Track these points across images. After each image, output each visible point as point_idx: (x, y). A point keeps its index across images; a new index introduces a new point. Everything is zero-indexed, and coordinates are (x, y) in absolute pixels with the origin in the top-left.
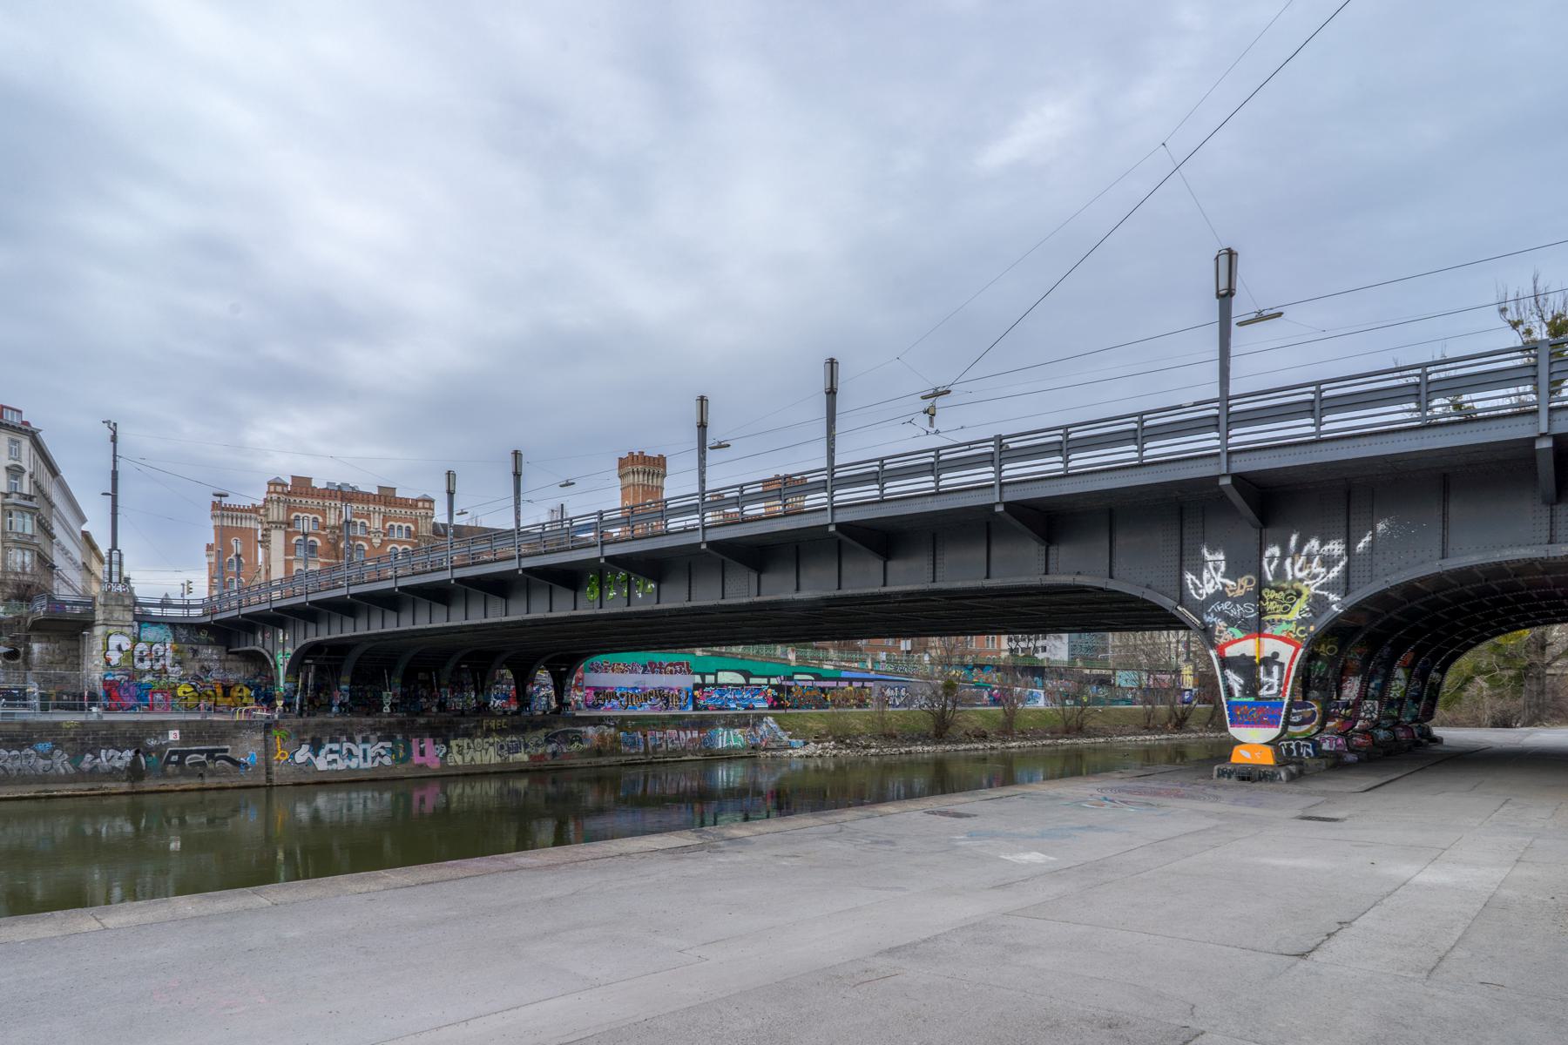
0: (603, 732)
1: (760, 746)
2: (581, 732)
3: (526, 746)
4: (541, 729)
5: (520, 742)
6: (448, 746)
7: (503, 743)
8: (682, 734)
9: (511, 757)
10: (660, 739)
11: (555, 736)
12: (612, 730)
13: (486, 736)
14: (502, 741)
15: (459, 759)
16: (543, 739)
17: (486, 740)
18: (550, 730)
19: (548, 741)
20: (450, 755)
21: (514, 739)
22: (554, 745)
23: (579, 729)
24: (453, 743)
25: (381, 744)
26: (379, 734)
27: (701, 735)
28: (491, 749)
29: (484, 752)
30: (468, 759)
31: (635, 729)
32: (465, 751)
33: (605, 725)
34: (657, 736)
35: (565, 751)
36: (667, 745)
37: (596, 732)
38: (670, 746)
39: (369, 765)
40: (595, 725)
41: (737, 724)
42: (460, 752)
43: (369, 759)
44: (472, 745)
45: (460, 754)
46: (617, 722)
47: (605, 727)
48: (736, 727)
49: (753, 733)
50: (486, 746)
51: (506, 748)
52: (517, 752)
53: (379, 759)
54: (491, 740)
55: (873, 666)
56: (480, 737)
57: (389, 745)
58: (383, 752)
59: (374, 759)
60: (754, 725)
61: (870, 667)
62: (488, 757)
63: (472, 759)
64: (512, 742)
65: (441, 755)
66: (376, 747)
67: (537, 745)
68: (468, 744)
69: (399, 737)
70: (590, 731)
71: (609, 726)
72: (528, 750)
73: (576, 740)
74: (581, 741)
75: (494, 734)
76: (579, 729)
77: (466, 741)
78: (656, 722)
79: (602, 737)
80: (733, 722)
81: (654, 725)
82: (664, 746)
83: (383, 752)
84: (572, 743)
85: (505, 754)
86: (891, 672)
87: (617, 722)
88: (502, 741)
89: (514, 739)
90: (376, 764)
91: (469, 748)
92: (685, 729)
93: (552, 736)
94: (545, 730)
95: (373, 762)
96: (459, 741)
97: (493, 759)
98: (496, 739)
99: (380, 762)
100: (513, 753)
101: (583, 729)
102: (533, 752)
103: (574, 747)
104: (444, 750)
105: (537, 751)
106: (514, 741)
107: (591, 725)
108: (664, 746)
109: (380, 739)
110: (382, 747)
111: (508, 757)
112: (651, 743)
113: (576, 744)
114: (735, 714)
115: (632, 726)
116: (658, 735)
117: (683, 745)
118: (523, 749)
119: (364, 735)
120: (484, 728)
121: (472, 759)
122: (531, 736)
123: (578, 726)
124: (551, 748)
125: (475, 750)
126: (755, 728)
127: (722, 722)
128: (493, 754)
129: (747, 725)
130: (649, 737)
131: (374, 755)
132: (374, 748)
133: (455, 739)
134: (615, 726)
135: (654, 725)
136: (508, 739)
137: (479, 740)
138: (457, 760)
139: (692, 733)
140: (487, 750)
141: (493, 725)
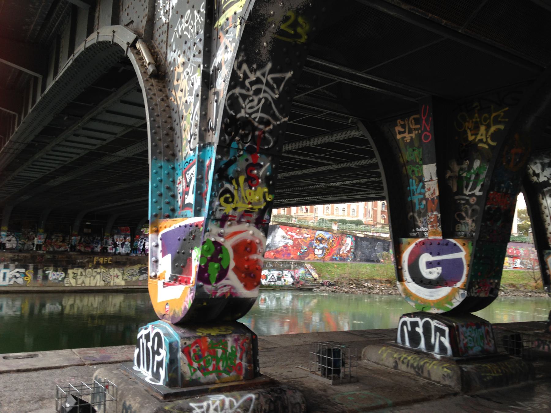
4: (136, 264)
6: (66, 273)
14: (107, 271)
15: (73, 282)
16: (138, 271)
17: (95, 270)
18: (143, 266)
20: (67, 279)
24: (70, 271)
25: (17, 270)
26: (16, 263)
28: (98, 276)
29: (92, 278)
30: (80, 282)
32: (78, 277)
39: (6, 283)
42: (75, 278)
43: (7, 279)
44: (84, 273)
45: (75, 279)
50: (95, 274)
53: (14, 279)
54: (98, 270)
56: (90, 268)
57: (23, 270)
58: (18, 275)
59: (11, 279)
63: (83, 282)
65: (60, 279)
66: (14, 271)
67: (133, 275)
68: (81, 272)
69: (31, 266)
75: (101, 267)
77: (80, 270)
83: (18, 275)
90: (12, 283)
91: (82, 275)
94: (139, 266)
95: (10, 281)
96: (75, 270)
97: (98, 282)
98: (102, 270)
99: (15, 281)
102: (129, 279)
104: (63, 275)
105: (132, 278)
109: (17, 267)
110: (18, 272)
119: (6, 263)
120: (95, 263)
121: (83, 282)
125: (86, 276)
127: (271, 265)
128: (99, 279)
131: (11, 276)
132: (11, 273)
133: (72, 268)
137: (90, 270)
138: (72, 283)
140: (95, 277)
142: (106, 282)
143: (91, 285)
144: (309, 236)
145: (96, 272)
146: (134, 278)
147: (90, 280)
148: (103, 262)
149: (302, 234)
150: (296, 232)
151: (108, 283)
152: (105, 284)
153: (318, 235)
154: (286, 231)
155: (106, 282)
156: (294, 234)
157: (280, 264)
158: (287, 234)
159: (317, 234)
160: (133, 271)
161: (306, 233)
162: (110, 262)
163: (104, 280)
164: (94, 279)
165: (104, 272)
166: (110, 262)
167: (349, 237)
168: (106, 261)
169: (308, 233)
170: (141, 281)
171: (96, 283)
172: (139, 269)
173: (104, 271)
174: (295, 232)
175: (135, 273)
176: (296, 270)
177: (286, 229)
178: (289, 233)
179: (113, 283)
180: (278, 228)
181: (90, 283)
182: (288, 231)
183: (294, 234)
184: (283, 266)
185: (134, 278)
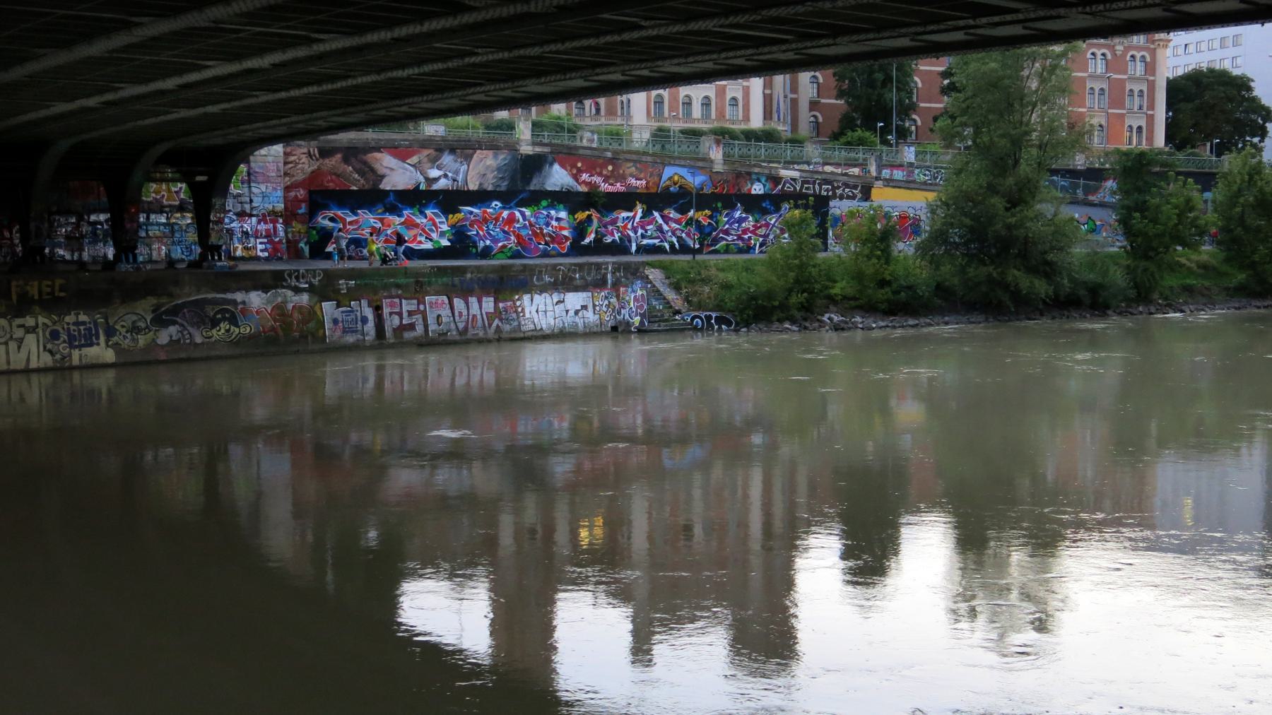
0: (285, 302)
1: (628, 324)
2: (234, 302)
3: (110, 332)
4: (144, 297)
5: (96, 324)
7: (58, 327)
8: (458, 303)
9: (76, 354)
10: (410, 313)
11: (176, 311)
12: (305, 298)
13: (20, 313)
14: (54, 323)
17: (19, 321)
18: (164, 300)
19: (160, 321)
21: (83, 318)
22: (173, 330)
23: (229, 296)
27: (501, 305)
28: (31, 339)
29: (13, 346)
31: (354, 295)
33: (289, 287)
34: (405, 309)
35: (198, 340)
36: (426, 326)
37: (268, 302)
38: (433, 327)
40: (265, 289)
41: (578, 282)
46: (316, 282)
47: (289, 293)
48: (576, 289)
49: (614, 300)
50: (19, 333)
51: (64, 337)
52: (91, 345)
54: (30, 321)
55: (879, 172)
60: (616, 285)
61: (874, 174)
62: (23, 355)
64: (77, 324)
67: (135, 329)
70: (256, 300)
71: (297, 290)
72: (115, 339)
73: (224, 319)
74: (233, 321)
75: (37, 309)
76: (229, 296)
78: (402, 281)
79: (280, 311)
80: (572, 279)
81: (398, 286)
82: (420, 329)
84: (215, 323)
85: (63, 348)
86: (925, 183)
87: (316, 282)
88: (54, 323)
89: (83, 318)
92: (465, 293)
93: (167, 312)
94: (152, 301)
97: (34, 359)
98: (41, 320)
100: (80, 347)
101: (239, 296)
102: (127, 343)
103: (219, 333)
105: (135, 340)
106: (84, 323)
107: (255, 288)
108: (420, 329)
111: (70, 355)
112: (392, 322)
113: (224, 326)
114: (575, 265)
115: (348, 289)
116: (407, 306)
117: (461, 326)
118: (102, 338)
120: (14, 297)
122: (122, 311)
123: (225, 291)
124: (164, 337)
126: (617, 291)
127: (547, 279)
129: (600, 284)
130: (386, 311)
134: (311, 290)
135: (398, 286)
136: (70, 319)
139: (480, 302)
140: (20, 341)
141: (33, 290)
142: (58, 356)
143: (12, 367)
144: (644, 182)
145: (20, 326)
146: (142, 340)
147: (7, 353)
148: (40, 293)
149: (622, 178)
150: (605, 172)
151: (63, 358)
152: (55, 361)
153: (670, 179)
154: (575, 171)
155: (58, 356)
156: (597, 179)
157: (575, 271)
158: (577, 180)
159: (665, 177)
160: (135, 318)
161: (633, 176)
162: (62, 294)
163: (50, 352)
164: (19, 347)
165: (44, 324)
166: (62, 294)
167: (759, 180)
168: (49, 290)
169: (642, 176)
170: (162, 346)
171: (28, 360)
172: (153, 311)
173: (46, 321)
174: (600, 174)
175: (142, 325)
176: (622, 289)
177: (574, 166)
178: (585, 177)
179: (80, 360)
180: (551, 165)
181: (8, 363)
182: (580, 171)
183: (597, 179)
184: (582, 278)
185: (142, 340)
